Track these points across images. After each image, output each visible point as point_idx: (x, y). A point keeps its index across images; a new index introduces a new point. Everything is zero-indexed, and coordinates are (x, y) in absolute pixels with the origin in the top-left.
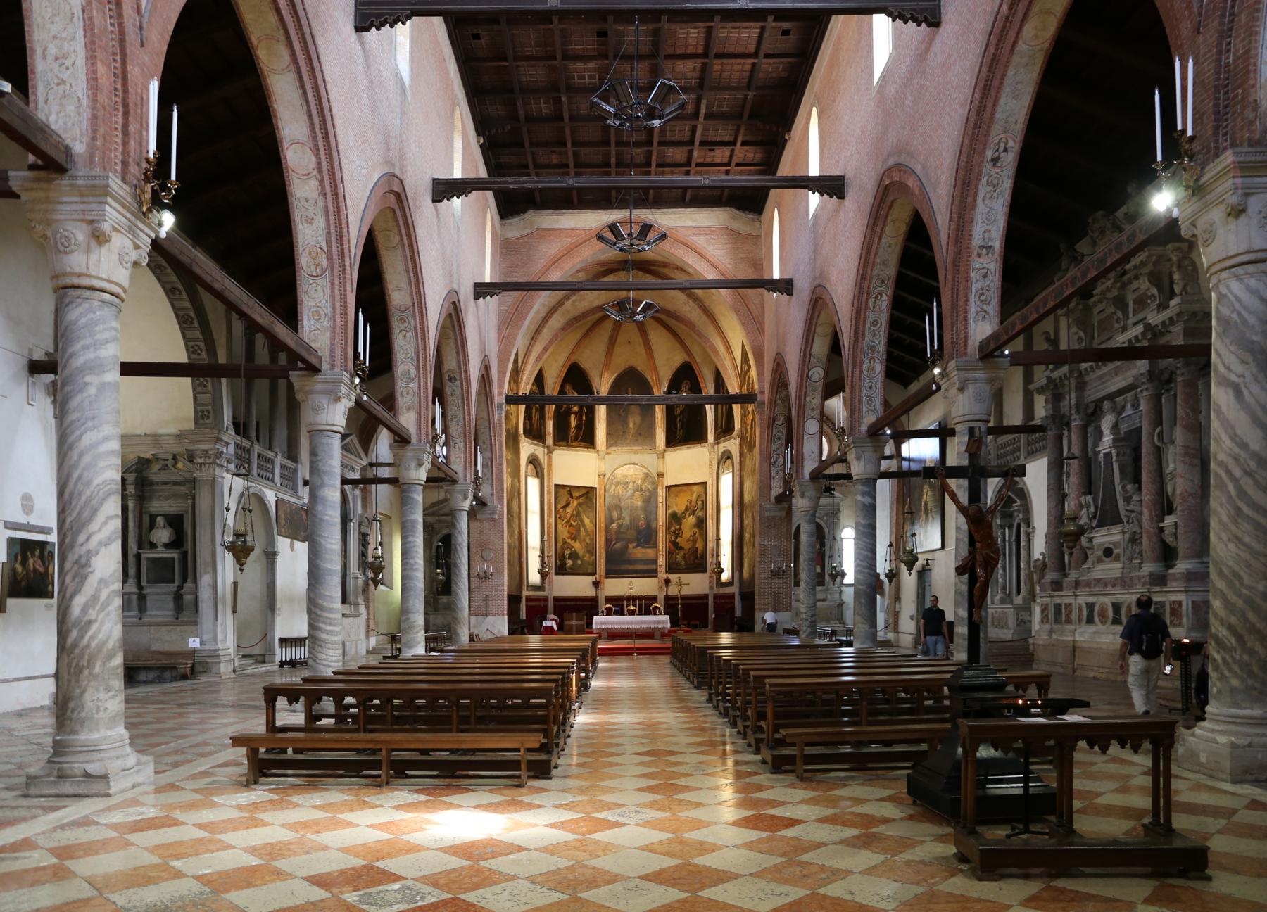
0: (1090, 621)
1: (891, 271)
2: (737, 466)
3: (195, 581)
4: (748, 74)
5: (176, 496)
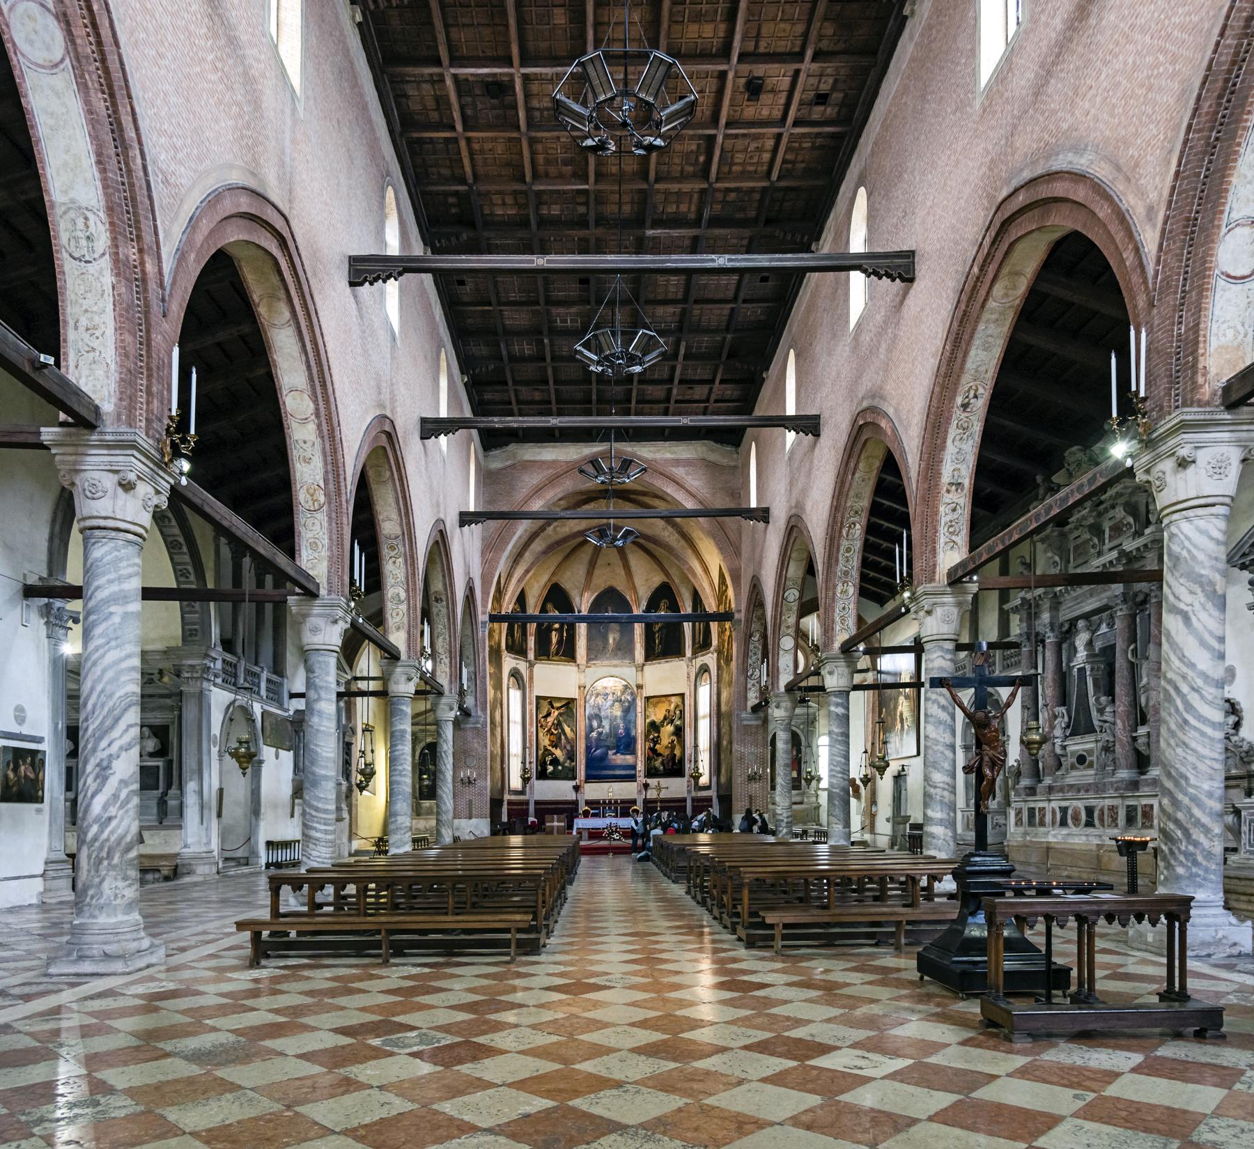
0: (1063, 823)
1: (865, 503)
2: (714, 679)
3: (180, 787)
5: (161, 708)
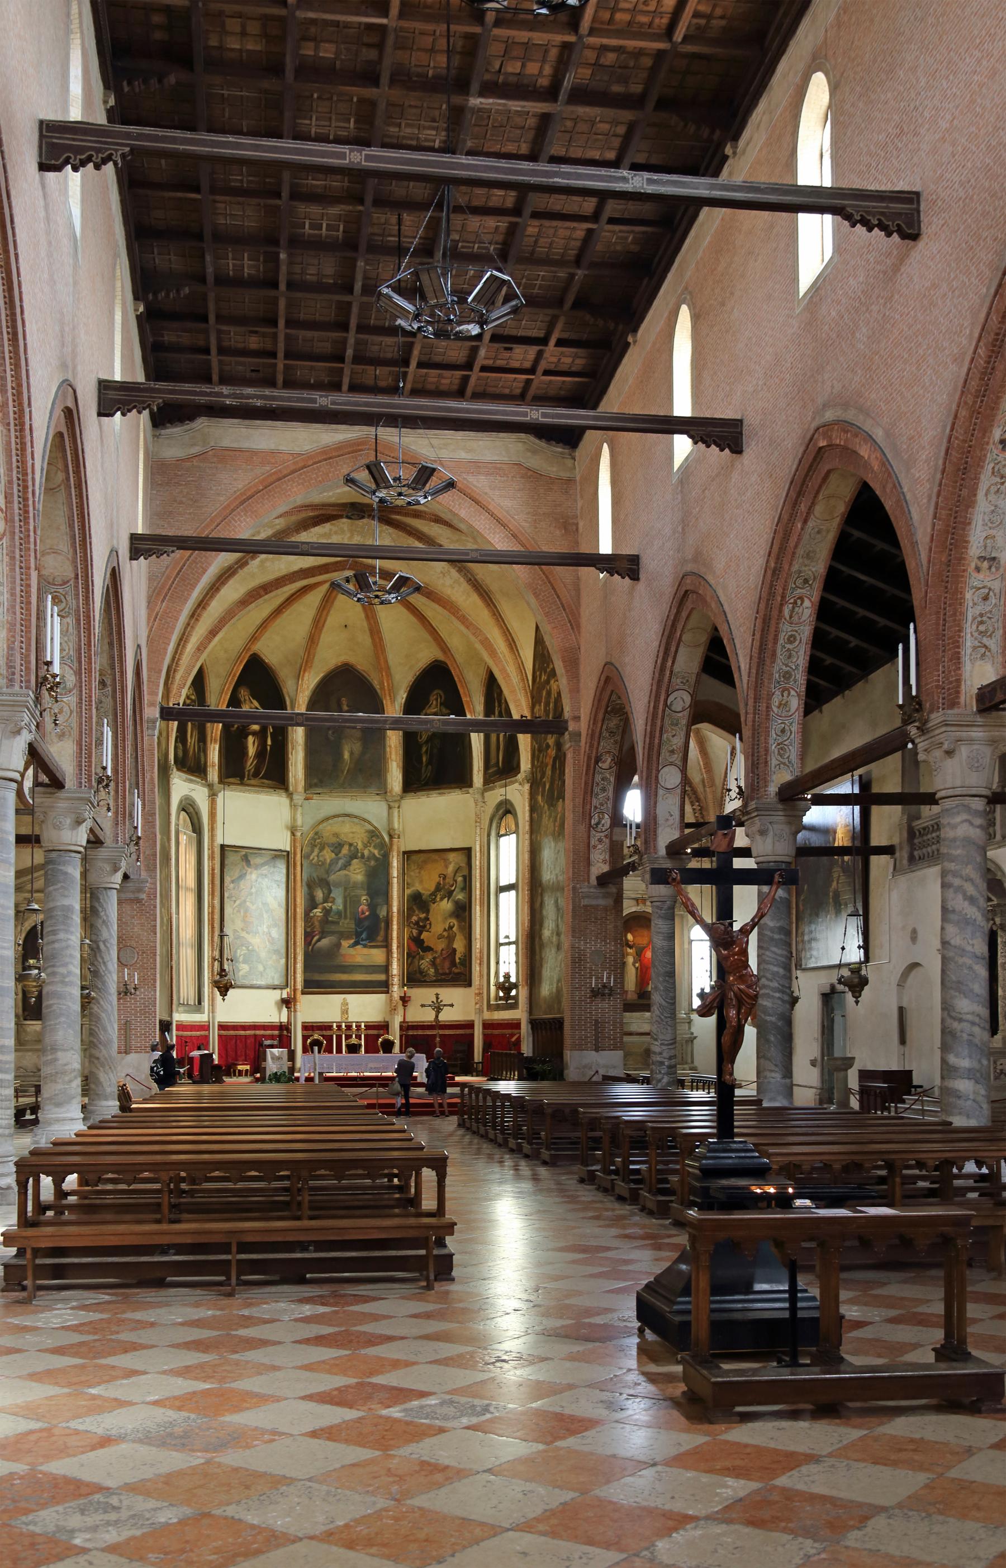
4: (578, 244)
